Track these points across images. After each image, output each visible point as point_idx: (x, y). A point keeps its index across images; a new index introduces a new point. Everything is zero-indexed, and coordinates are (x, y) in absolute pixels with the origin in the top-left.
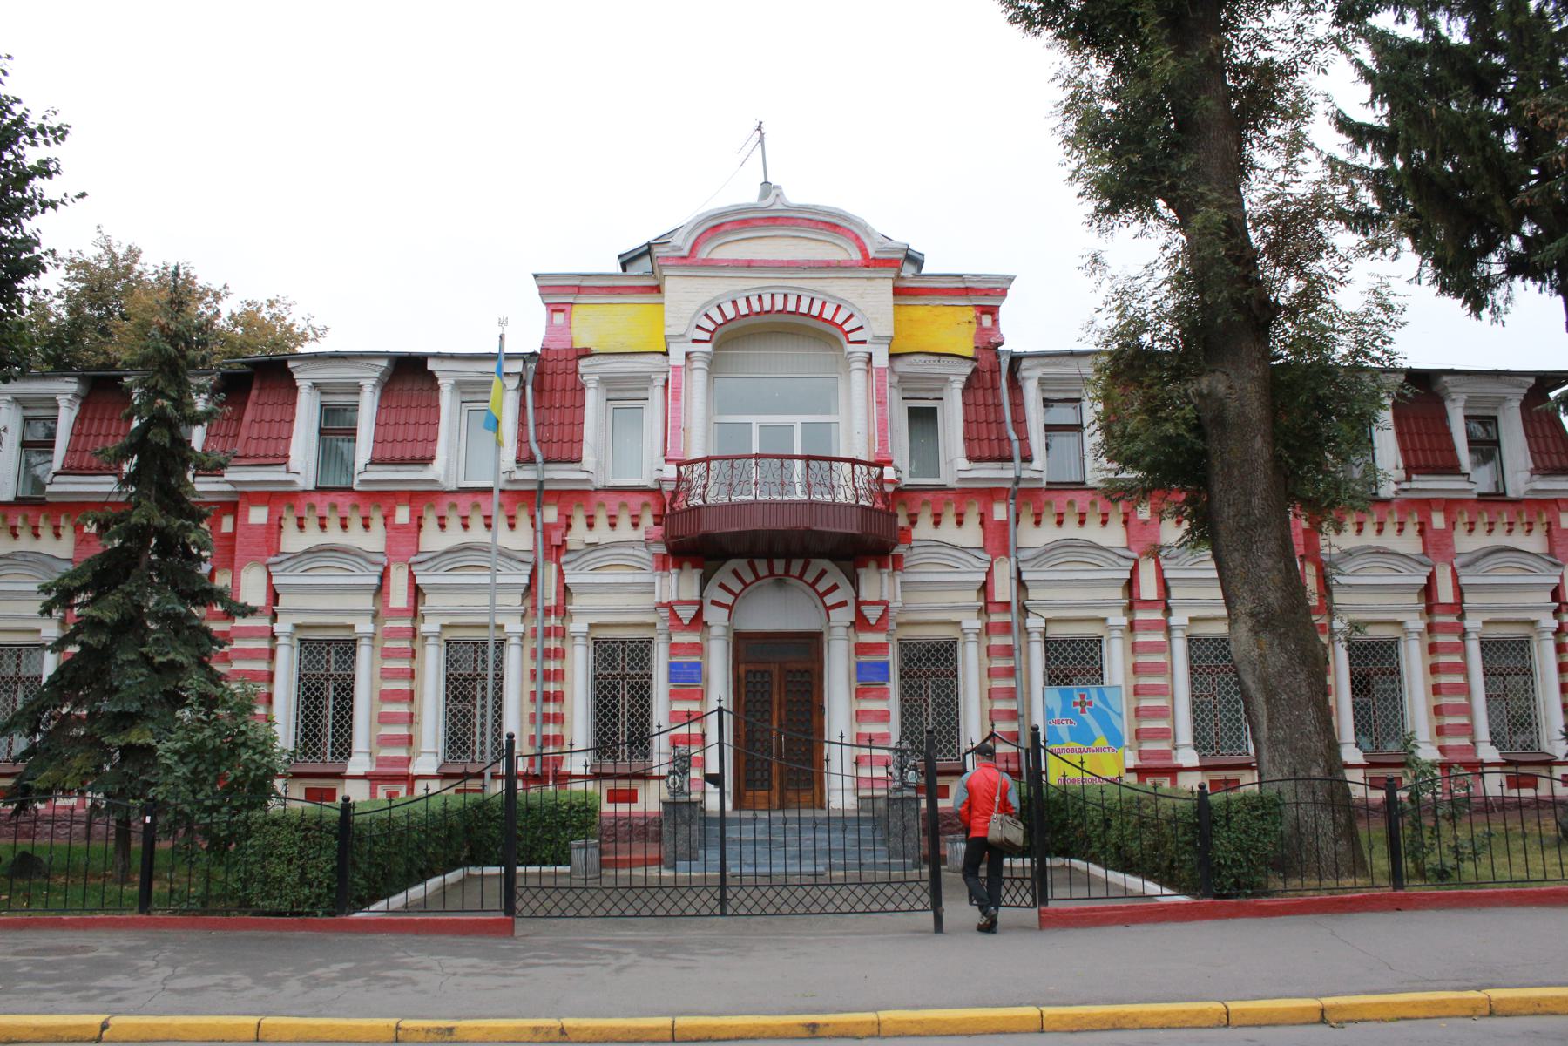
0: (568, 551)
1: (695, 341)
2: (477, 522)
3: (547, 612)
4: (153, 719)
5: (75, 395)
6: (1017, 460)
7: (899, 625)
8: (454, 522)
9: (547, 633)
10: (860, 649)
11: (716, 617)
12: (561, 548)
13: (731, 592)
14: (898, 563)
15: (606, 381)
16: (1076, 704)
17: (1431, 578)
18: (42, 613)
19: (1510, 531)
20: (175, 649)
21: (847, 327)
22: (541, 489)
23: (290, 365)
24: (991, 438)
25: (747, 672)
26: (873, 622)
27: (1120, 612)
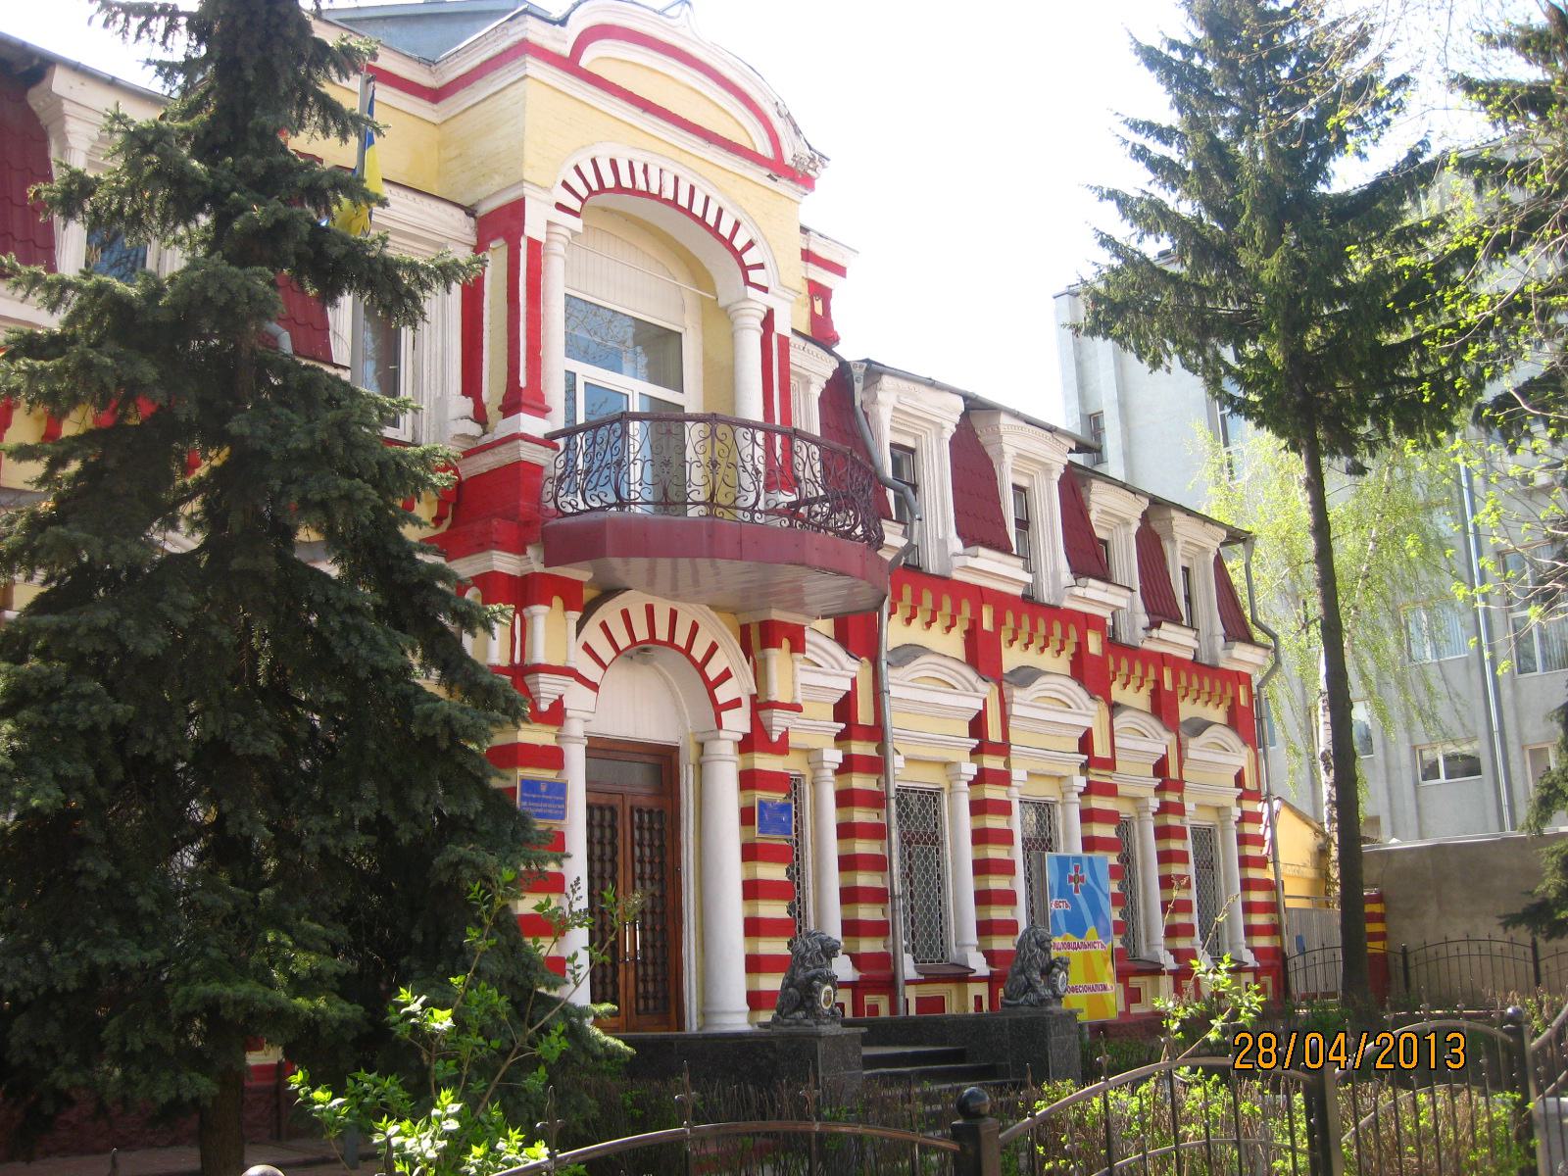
1: (560, 207)
26: (775, 738)
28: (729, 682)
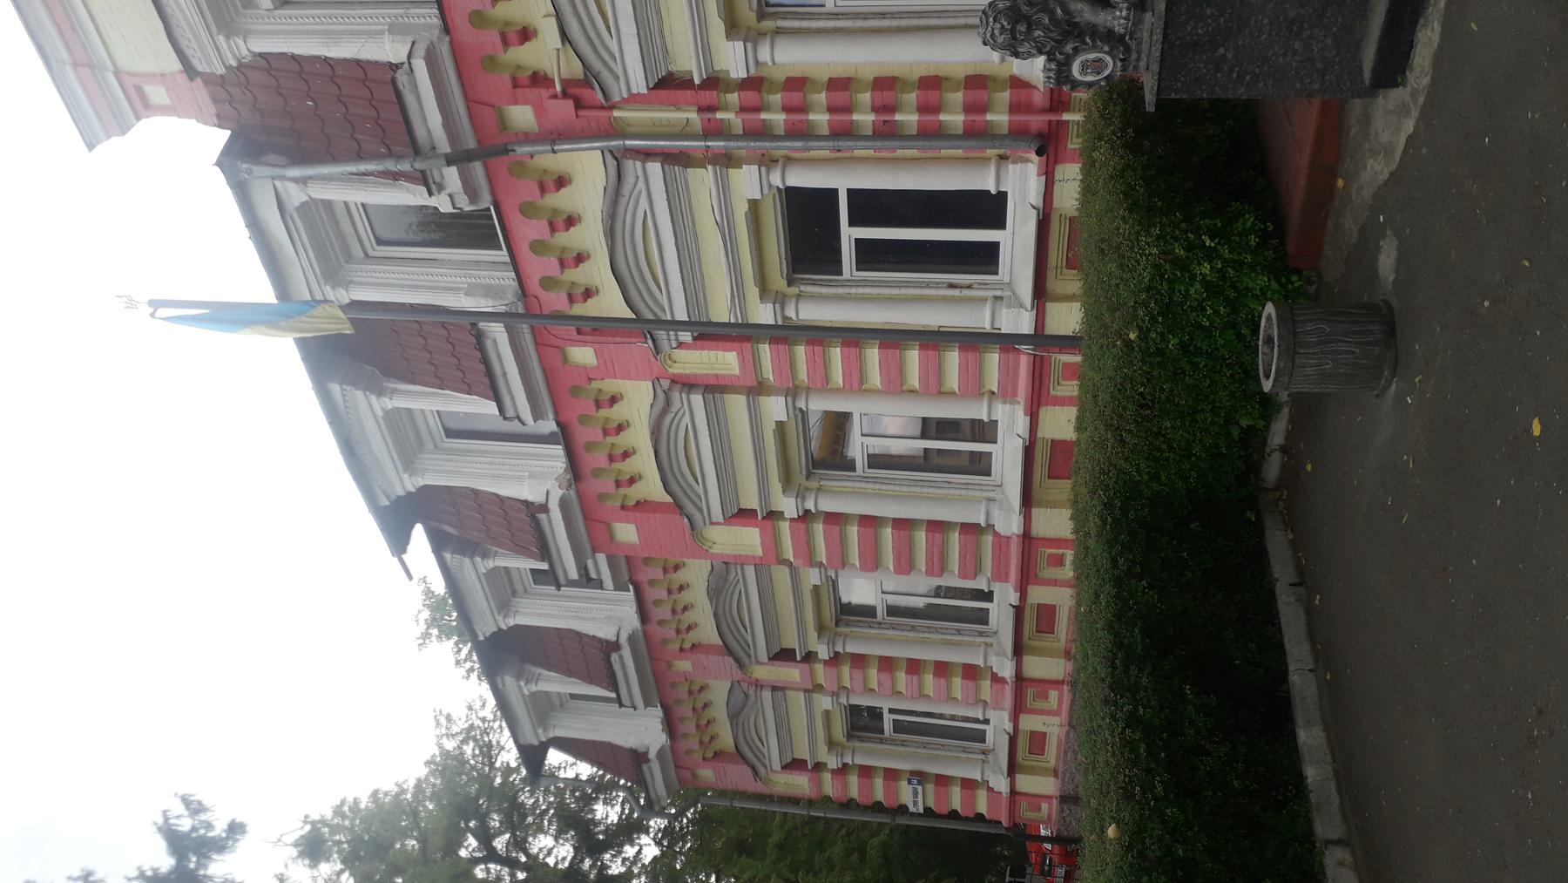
5: (518, 677)
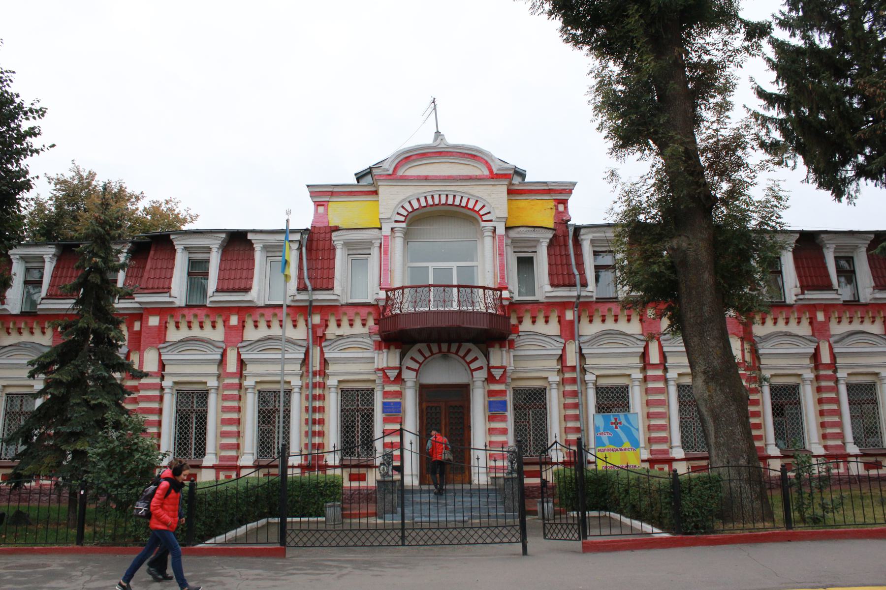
0: (326, 340)
1: (396, 221)
2: (275, 324)
3: (315, 374)
4: (89, 436)
5: (54, 255)
6: (579, 286)
7: (512, 379)
8: (262, 324)
9: (315, 386)
10: (491, 393)
11: (409, 376)
12: (323, 338)
13: (417, 362)
14: (511, 345)
15: (347, 244)
16: (612, 423)
17: (817, 349)
18: (29, 377)
19: (862, 322)
20: (102, 396)
21: (481, 212)
22: (311, 305)
23: (172, 237)
24: (561, 275)
25: (427, 407)
26: (497, 378)
27: (638, 371)
28: (477, 362)
